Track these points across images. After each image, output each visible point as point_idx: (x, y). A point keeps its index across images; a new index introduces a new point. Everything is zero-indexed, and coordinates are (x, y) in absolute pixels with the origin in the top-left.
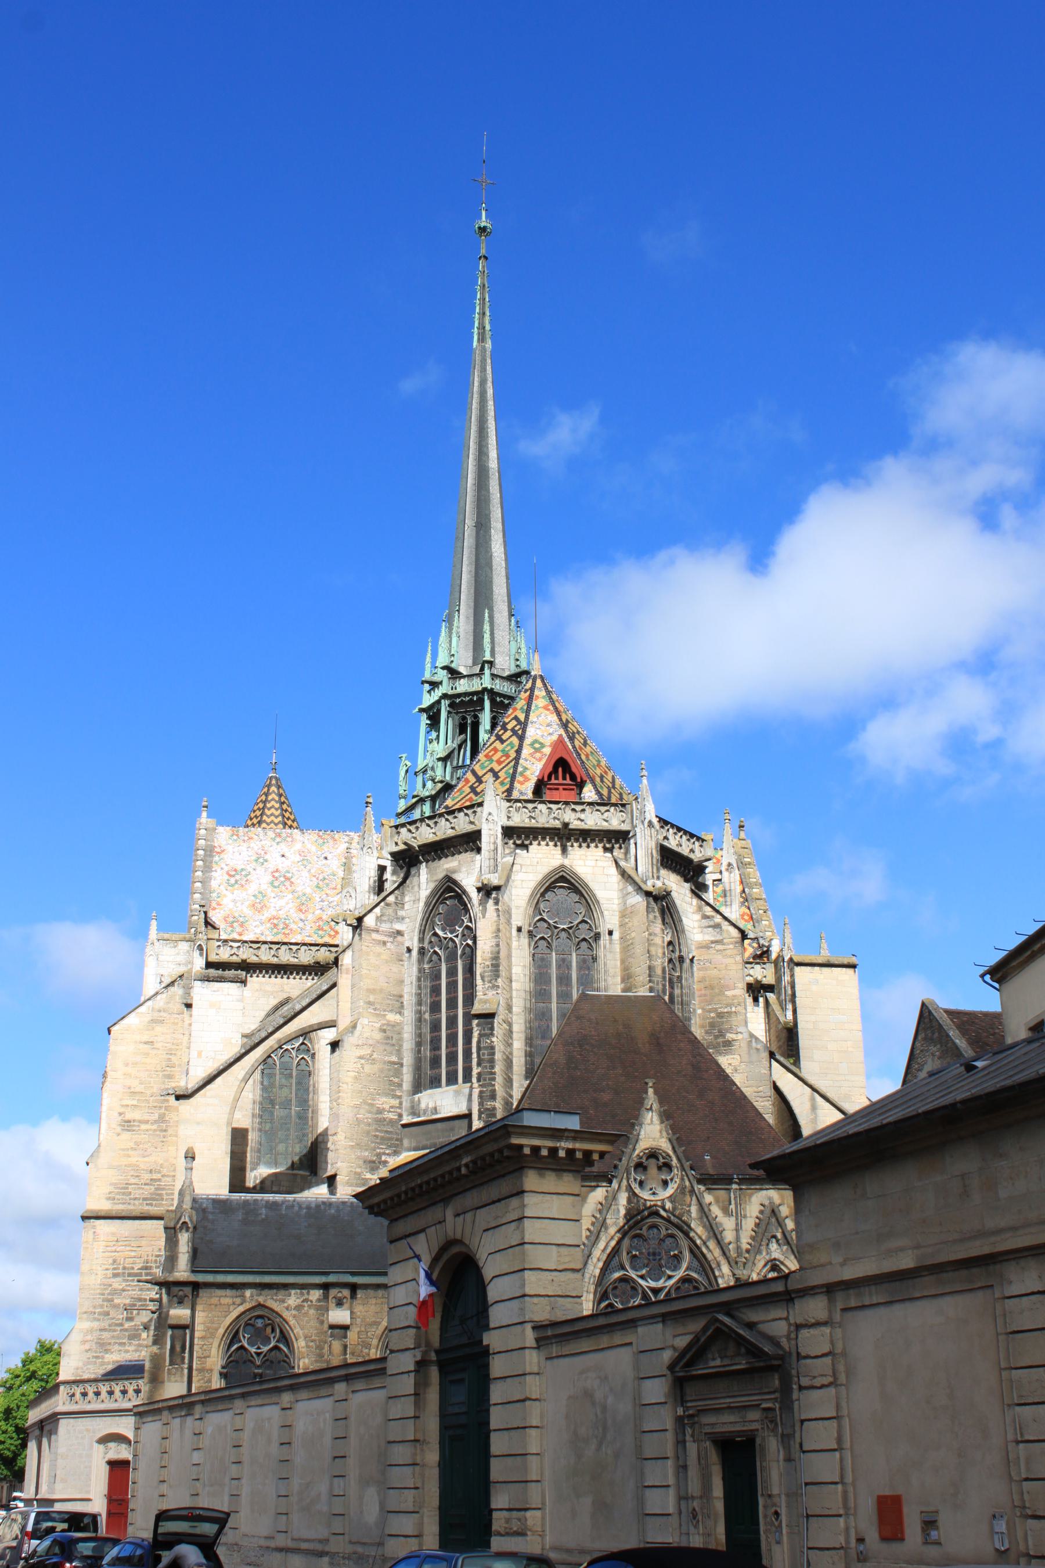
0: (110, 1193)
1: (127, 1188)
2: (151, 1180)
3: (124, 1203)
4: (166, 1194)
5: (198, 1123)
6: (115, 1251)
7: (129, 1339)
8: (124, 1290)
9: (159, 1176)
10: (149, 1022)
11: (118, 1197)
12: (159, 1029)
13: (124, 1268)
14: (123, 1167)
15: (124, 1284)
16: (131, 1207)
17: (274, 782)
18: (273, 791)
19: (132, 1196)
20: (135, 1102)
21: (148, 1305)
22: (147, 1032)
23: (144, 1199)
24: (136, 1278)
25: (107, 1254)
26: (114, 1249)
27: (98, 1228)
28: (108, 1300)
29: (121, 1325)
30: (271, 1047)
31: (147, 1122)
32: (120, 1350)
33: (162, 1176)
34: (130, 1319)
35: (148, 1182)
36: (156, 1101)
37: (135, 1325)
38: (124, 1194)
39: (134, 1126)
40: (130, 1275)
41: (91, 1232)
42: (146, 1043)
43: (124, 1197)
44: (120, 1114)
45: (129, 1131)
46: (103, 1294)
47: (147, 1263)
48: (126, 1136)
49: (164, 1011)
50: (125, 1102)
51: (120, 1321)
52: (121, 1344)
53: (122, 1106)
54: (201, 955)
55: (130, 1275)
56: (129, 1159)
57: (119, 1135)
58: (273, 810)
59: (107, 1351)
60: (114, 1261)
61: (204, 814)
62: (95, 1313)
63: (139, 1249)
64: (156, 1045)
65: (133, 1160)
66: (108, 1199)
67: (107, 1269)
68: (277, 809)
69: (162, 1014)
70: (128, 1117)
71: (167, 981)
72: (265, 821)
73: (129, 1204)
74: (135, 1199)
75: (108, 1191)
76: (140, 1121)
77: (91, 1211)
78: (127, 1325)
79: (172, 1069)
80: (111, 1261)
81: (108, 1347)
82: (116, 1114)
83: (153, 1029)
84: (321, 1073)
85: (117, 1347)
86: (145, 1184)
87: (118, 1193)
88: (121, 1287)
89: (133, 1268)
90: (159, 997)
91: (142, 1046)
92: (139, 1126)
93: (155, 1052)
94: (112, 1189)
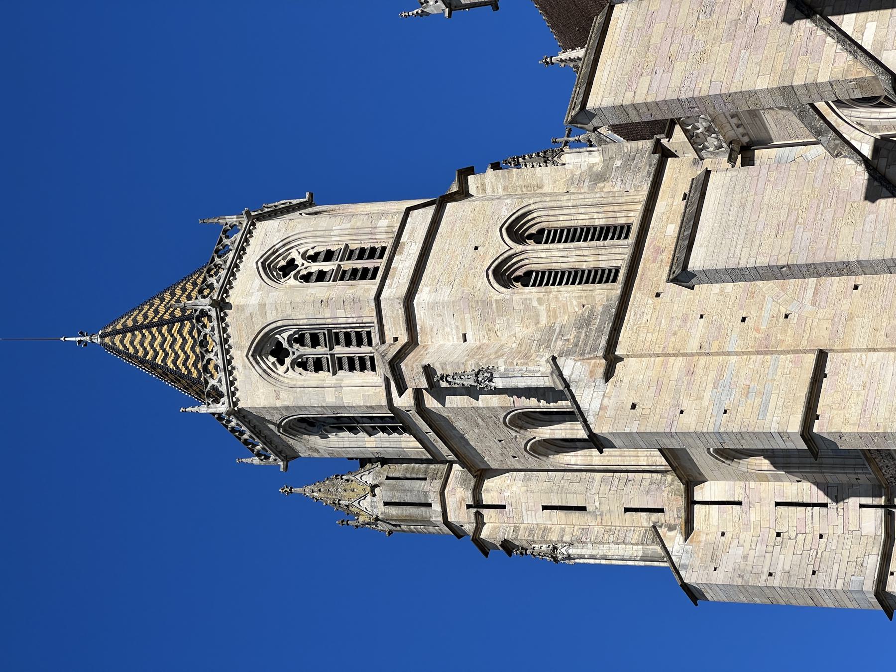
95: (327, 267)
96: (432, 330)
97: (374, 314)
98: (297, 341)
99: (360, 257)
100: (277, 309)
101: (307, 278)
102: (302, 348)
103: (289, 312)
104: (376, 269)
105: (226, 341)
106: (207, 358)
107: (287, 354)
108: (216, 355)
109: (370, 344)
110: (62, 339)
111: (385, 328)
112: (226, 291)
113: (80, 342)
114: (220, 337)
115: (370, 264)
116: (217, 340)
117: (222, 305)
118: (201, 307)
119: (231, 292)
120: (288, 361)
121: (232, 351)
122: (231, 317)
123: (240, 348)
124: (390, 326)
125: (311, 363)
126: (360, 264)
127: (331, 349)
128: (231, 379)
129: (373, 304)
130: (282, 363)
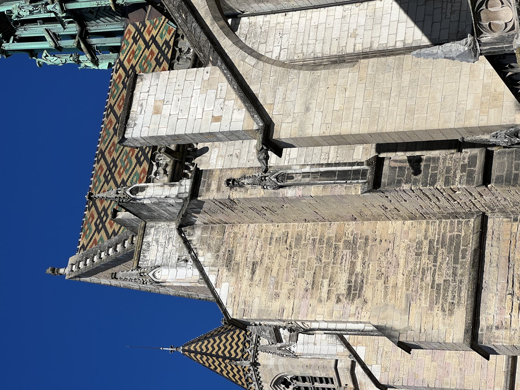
0: (443, 310)
1: (439, 285)
2: (430, 253)
4: (450, 232)
5: (307, 109)
9: (426, 243)
10: (229, 270)
11: (449, 300)
12: (238, 257)
14: (410, 292)
16: (466, 279)
17: (186, 348)
18: (195, 347)
19: (451, 279)
20: (326, 282)
22: (241, 271)
23: (456, 261)
27: (491, 322)
30: (222, 28)
31: (353, 264)
35: (432, 257)
36: (327, 255)
38: (446, 290)
39: (355, 281)
41: (497, 333)
42: (253, 272)
43: (451, 289)
44: (339, 300)
45: (362, 287)
48: (368, 292)
49: (218, 251)
50: (324, 295)
53: (328, 298)
54: (143, 189)
56: (399, 285)
57: (365, 302)
58: (209, 346)
61: (62, 271)
64: (258, 259)
66: (451, 312)
68: (209, 342)
69: (221, 253)
70: (342, 289)
71: (185, 254)
72: (217, 352)
73: (461, 282)
74: (454, 274)
75: (440, 313)
76: (351, 274)
77: (466, 332)
79: (289, 235)
82: (340, 305)
83: (238, 264)
84: (320, 55)
86: (435, 261)
87: (445, 299)
90: (201, 259)
91: (256, 277)
92: (357, 275)
93: (266, 260)
94: (437, 309)
96: (365, 383)
97: (335, 373)
98: (294, 379)
100: (284, 368)
102: (297, 382)
103: (291, 369)
105: (259, 379)
106: (250, 386)
108: (255, 385)
109: (333, 383)
110: (161, 349)
111: (341, 380)
112: (256, 357)
113: (171, 351)
114: (256, 378)
116: (255, 380)
117: (255, 364)
118: (245, 365)
119: (258, 357)
121: (262, 384)
122: (260, 369)
123: (266, 382)
124: (343, 379)
127: (313, 384)
128: (261, 387)
129: (334, 370)
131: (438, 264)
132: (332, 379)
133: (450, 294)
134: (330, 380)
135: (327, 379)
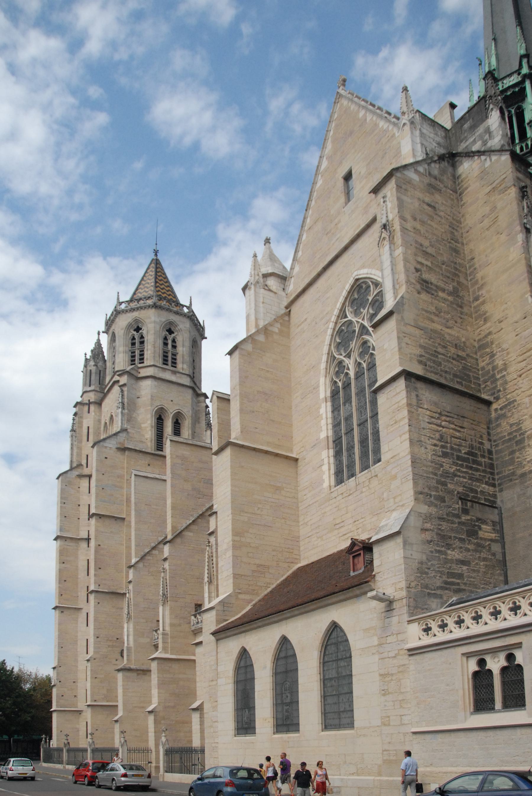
3: (436, 374)
6: (440, 426)
7: (468, 536)
8: (456, 475)
13: (452, 448)
15: (454, 468)
21: (479, 498)
24: (465, 464)
25: (433, 426)
26: (439, 422)
28: (444, 484)
29: (457, 516)
32: (461, 548)
33: (467, 355)
34: (466, 511)
35: (455, 356)
37: (471, 520)
40: (458, 458)
46: (436, 474)
47: (473, 448)
51: (456, 512)
52: (462, 540)
55: (458, 458)
59: (449, 546)
60: (442, 437)
62: (431, 496)
63: (462, 430)
65: (438, 327)
67: (435, 445)
73: (441, 376)
78: (464, 518)
80: (437, 436)
81: (449, 541)
85: (457, 543)
88: (452, 470)
89: (460, 451)
95: (170, 346)
99: (173, 358)
101: (166, 338)
104: (167, 365)
107: (138, 332)
115: (170, 363)
120: (135, 333)
125: (134, 341)
126: (170, 359)
130: (135, 330)
131: (452, 361)
132: (143, 363)
133: (432, 364)
134: (142, 361)
135: (143, 359)
